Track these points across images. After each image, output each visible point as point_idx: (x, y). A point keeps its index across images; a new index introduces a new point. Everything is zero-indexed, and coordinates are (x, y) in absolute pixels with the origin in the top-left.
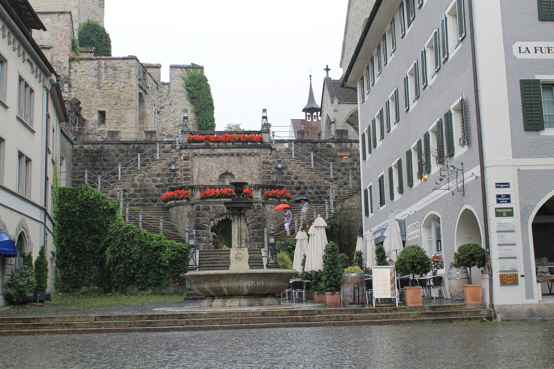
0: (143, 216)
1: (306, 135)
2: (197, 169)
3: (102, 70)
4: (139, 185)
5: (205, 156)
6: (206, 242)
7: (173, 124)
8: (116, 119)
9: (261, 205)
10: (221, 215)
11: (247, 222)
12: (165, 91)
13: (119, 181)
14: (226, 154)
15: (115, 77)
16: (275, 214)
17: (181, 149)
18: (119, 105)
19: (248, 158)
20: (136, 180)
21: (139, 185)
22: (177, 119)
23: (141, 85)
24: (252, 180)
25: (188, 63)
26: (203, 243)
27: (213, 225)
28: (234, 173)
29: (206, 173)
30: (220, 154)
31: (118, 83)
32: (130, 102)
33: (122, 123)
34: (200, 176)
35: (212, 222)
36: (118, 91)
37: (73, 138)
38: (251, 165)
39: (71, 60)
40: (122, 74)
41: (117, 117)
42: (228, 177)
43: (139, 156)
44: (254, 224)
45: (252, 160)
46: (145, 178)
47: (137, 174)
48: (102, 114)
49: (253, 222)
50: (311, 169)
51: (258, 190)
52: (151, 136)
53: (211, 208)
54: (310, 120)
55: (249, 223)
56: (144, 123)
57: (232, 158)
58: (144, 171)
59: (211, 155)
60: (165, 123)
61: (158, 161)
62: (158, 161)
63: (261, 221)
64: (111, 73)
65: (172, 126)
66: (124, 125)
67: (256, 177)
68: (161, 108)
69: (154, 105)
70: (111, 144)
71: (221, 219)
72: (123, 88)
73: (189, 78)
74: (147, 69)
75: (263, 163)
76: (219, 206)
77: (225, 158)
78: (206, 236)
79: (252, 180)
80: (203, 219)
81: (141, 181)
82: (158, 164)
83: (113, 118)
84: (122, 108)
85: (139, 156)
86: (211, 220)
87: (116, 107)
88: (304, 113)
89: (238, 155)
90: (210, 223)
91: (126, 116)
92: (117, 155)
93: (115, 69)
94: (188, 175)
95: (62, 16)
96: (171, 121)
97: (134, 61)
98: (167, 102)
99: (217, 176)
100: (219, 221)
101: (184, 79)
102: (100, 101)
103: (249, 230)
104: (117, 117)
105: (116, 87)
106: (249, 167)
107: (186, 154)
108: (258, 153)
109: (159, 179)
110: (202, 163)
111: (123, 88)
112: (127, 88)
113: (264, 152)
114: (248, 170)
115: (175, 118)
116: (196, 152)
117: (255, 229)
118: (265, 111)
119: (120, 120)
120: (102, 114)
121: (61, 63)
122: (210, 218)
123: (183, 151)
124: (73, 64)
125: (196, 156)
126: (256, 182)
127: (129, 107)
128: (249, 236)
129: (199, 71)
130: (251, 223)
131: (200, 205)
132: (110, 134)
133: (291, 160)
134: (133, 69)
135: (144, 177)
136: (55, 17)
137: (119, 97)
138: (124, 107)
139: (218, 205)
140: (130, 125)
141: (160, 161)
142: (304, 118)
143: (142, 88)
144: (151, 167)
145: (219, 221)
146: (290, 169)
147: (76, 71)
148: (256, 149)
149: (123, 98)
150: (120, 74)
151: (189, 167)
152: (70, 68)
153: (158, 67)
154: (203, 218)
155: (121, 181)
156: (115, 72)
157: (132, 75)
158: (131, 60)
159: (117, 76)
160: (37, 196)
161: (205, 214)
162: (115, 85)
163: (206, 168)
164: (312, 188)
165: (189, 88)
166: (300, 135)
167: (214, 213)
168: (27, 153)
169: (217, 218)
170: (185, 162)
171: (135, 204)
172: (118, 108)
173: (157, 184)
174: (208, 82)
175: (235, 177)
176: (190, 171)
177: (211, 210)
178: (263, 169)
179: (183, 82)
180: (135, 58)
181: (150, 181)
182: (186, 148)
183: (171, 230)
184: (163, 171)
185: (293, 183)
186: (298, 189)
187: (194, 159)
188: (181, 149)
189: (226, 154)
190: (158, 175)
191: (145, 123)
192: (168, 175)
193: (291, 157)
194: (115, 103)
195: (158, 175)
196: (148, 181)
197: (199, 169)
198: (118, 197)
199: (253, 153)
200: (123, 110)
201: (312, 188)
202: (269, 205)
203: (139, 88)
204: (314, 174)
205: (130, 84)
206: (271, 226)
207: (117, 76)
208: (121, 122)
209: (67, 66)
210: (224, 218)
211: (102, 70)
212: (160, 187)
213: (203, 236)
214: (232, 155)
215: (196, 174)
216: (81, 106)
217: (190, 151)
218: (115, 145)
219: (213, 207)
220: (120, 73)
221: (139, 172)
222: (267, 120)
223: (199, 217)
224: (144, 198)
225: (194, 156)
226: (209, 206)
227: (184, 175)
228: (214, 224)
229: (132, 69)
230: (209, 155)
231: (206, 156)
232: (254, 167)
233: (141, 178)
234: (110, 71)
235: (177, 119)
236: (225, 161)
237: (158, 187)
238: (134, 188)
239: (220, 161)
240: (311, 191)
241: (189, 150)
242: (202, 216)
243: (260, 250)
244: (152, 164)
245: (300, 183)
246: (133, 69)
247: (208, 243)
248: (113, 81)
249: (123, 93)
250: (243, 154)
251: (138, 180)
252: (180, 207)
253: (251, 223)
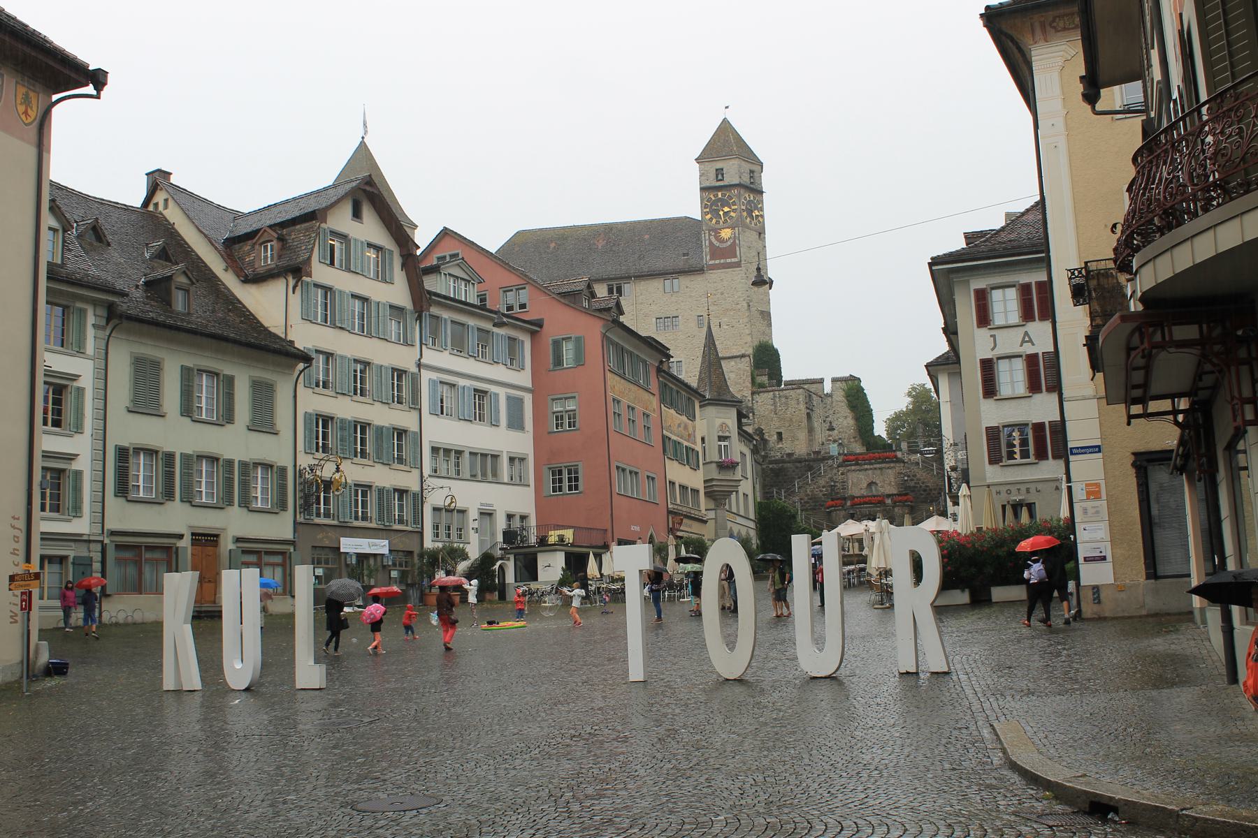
3: (777, 400)
12: (829, 402)
15: (786, 404)
25: (847, 375)
31: (790, 409)
37: (761, 460)
39: (753, 393)
48: (780, 434)
66: (796, 442)
68: (826, 417)
73: (849, 389)
87: (790, 428)
91: (798, 435)
93: (787, 398)
95: (743, 359)
98: (831, 412)
101: (844, 390)
102: (777, 424)
119: (794, 439)
120: (780, 434)
121: (746, 397)
124: (754, 397)
129: (856, 382)
134: (801, 396)
136: (738, 360)
147: (757, 402)
152: (753, 400)
153: (821, 381)
160: (752, 516)
164: (935, 489)
165: (848, 398)
168: (746, 493)
174: (865, 391)
179: (843, 393)
185: (921, 486)
209: (750, 399)
211: (777, 400)
216: (764, 431)
234: (783, 400)
235: (840, 426)
246: (801, 396)
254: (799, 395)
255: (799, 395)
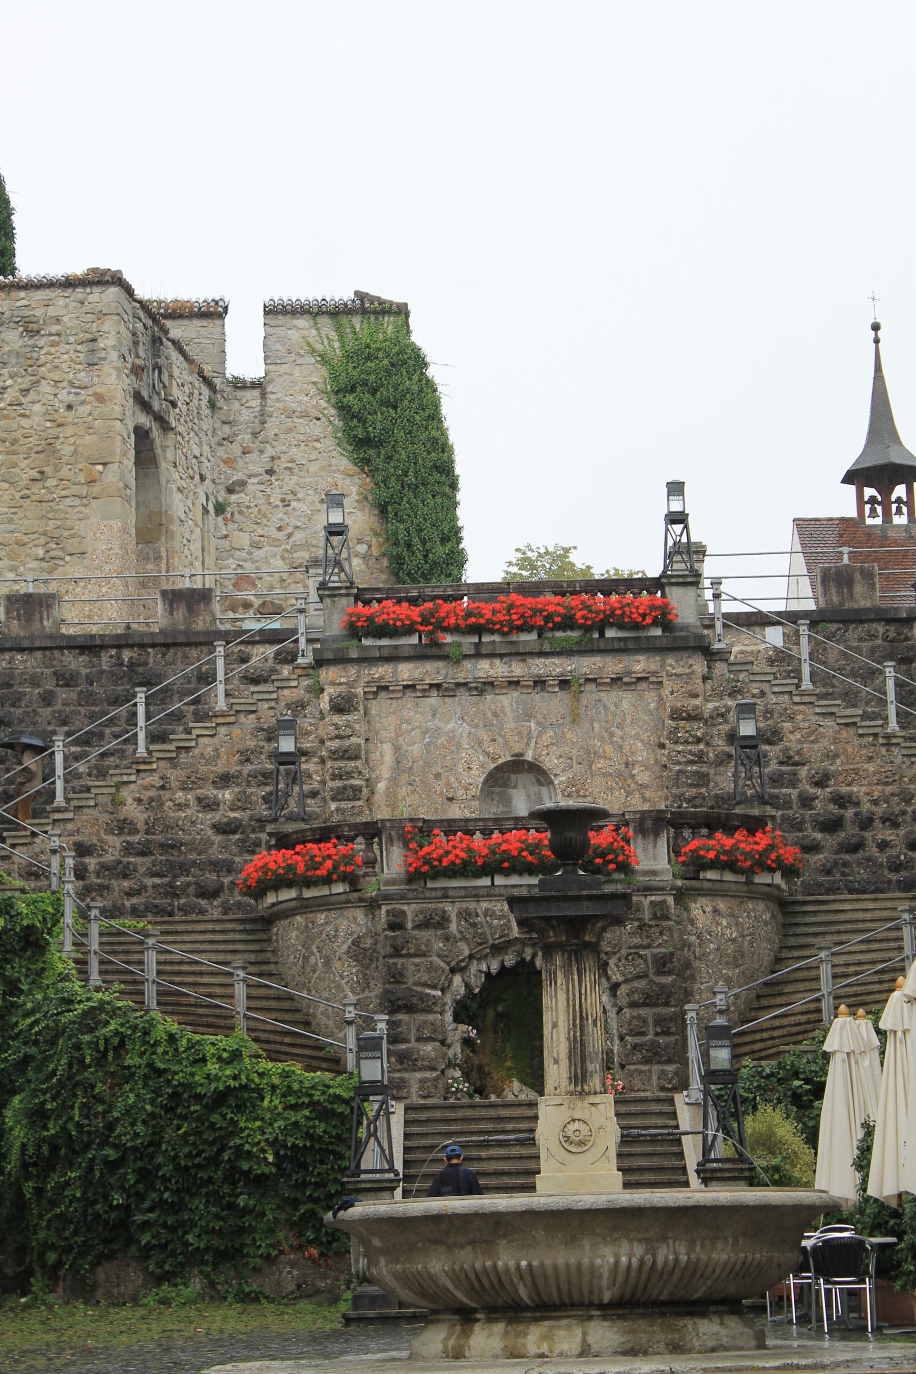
0: (162, 957)
1: (858, 589)
2: (387, 750)
4: (141, 826)
5: (424, 690)
6: (433, 1069)
7: (283, 558)
8: (42, 540)
9: (670, 900)
10: (497, 949)
11: (608, 979)
12: (246, 416)
13: (58, 810)
14: (514, 684)
15: (31, 364)
16: (733, 940)
17: (320, 663)
18: (51, 483)
19: (610, 697)
20: (130, 801)
21: (141, 826)
22: (298, 536)
23: (145, 394)
24: (629, 794)
25: (343, 293)
26: (420, 1070)
27: (462, 990)
28: (550, 762)
29: (428, 764)
30: (484, 683)
31: (45, 387)
32: (100, 468)
33: (68, 558)
34: (404, 778)
35: (457, 980)
36: (48, 424)
38: (621, 726)
40: (63, 348)
41: (45, 534)
42: (524, 777)
43: (141, 698)
44: (641, 984)
45: (625, 705)
46: (166, 795)
47: (133, 778)
49: (639, 977)
50: (888, 737)
51: (657, 835)
52: (190, 609)
53: (454, 918)
54: (878, 521)
55: (620, 978)
56: (158, 558)
57: (537, 698)
58: (162, 764)
59: (447, 689)
60: (250, 553)
61: (220, 720)
62: (220, 720)
63: (670, 973)
64: (16, 347)
65: (278, 564)
66: (74, 569)
67: (644, 777)
68: (230, 490)
69: (202, 478)
70: (21, 650)
71: (495, 967)
72: (70, 407)
73: (349, 357)
74: (168, 323)
75: (676, 715)
76: (487, 910)
77: (508, 701)
78: (433, 1040)
79: (629, 794)
80: (417, 965)
81: (153, 804)
82: (223, 730)
83: (25, 539)
84: (63, 493)
85: (141, 698)
86: (453, 971)
87: (38, 491)
88: (853, 488)
89: (564, 684)
90: (451, 982)
92: (47, 699)
93: (31, 329)
94: (349, 775)
96: (275, 543)
97: (113, 291)
98: (256, 464)
99: (478, 777)
100: (488, 974)
101: (324, 359)
103: (620, 1010)
104: (45, 534)
105: (37, 408)
106: (612, 735)
107: (340, 684)
108: (653, 673)
109: (227, 795)
110: (407, 721)
111: (70, 407)
112: (83, 410)
113: (679, 670)
114: (609, 749)
115: (290, 530)
116: (381, 678)
117: (645, 1005)
118: (676, 489)
122: (448, 963)
123: (328, 674)
125: (383, 694)
126: (645, 800)
127: (96, 489)
128: (622, 1038)
129: (389, 324)
130: (626, 981)
131: (405, 908)
132: (18, 610)
133: (797, 699)
134: (109, 325)
135: (163, 788)
137: (49, 447)
138: (74, 490)
139: (484, 905)
140: (100, 568)
141: (232, 719)
142: (853, 513)
143: (144, 405)
144: (193, 744)
145: (488, 974)
146: (792, 740)
148: (641, 658)
149: (66, 450)
150: (53, 350)
151: (354, 740)
154: (417, 960)
155: (66, 810)
156: (32, 342)
157: (103, 354)
158: (97, 290)
159: (43, 359)
161: (428, 944)
162: (32, 396)
163: (429, 744)
165: (350, 399)
166: (833, 590)
167: (463, 938)
169: (479, 959)
170: (337, 719)
171: (127, 904)
172: (50, 497)
173: (217, 817)
174: (431, 372)
175: (551, 782)
176: (356, 758)
177: (453, 927)
178: (676, 743)
179: (320, 375)
180: (116, 280)
181: (187, 806)
182: (341, 660)
183: (280, 1016)
184: (241, 763)
185: (806, 801)
186: (832, 825)
187: (375, 707)
188: (320, 663)
189: (514, 684)
190: (225, 780)
191: (164, 554)
192: (265, 777)
193: (798, 686)
194: (34, 474)
195: (225, 780)
196: (180, 807)
197: (397, 749)
198: (54, 880)
199: (629, 673)
200: (69, 501)
201: (891, 821)
202: (703, 901)
203: (137, 408)
204: (898, 760)
205: (99, 390)
206: (714, 993)
207: (43, 359)
208: (61, 554)
210: (510, 960)
212: (234, 832)
213: (419, 1040)
214: (540, 683)
215: (385, 771)
217: (358, 672)
218: (38, 654)
219: (460, 914)
220: (53, 344)
221: (140, 766)
222: (686, 527)
223: (402, 956)
224: (165, 880)
225: (376, 694)
226: (444, 911)
227: (334, 777)
228: (468, 986)
229: (105, 328)
230: (438, 686)
231: (425, 693)
232: (637, 737)
233: (153, 793)
235: (298, 536)
236: (508, 710)
237: (223, 829)
238: (123, 838)
239: (489, 714)
240: (887, 834)
241: (352, 670)
242: (416, 955)
243: (671, 1101)
244: (196, 732)
245: (841, 801)
246: (109, 325)
247: (443, 1072)
248: (25, 382)
249: (69, 431)
250: (587, 680)
251: (139, 801)
252: (321, 918)
253: (626, 981)
254: (101, 315)
255: (101, 315)
